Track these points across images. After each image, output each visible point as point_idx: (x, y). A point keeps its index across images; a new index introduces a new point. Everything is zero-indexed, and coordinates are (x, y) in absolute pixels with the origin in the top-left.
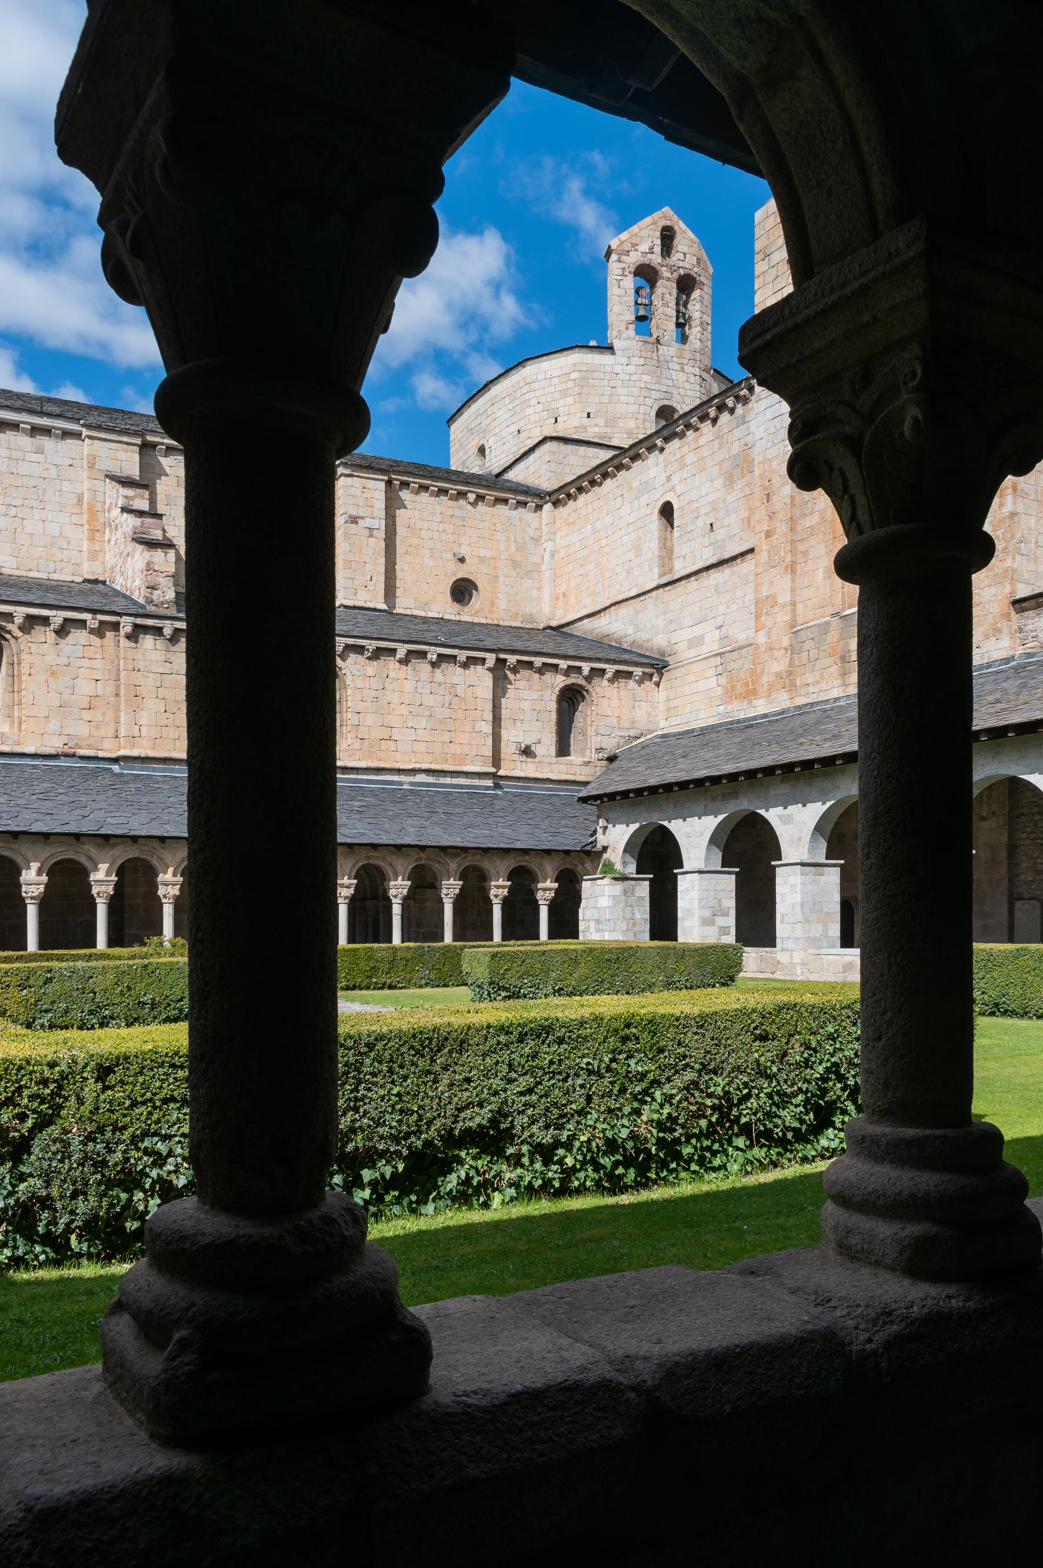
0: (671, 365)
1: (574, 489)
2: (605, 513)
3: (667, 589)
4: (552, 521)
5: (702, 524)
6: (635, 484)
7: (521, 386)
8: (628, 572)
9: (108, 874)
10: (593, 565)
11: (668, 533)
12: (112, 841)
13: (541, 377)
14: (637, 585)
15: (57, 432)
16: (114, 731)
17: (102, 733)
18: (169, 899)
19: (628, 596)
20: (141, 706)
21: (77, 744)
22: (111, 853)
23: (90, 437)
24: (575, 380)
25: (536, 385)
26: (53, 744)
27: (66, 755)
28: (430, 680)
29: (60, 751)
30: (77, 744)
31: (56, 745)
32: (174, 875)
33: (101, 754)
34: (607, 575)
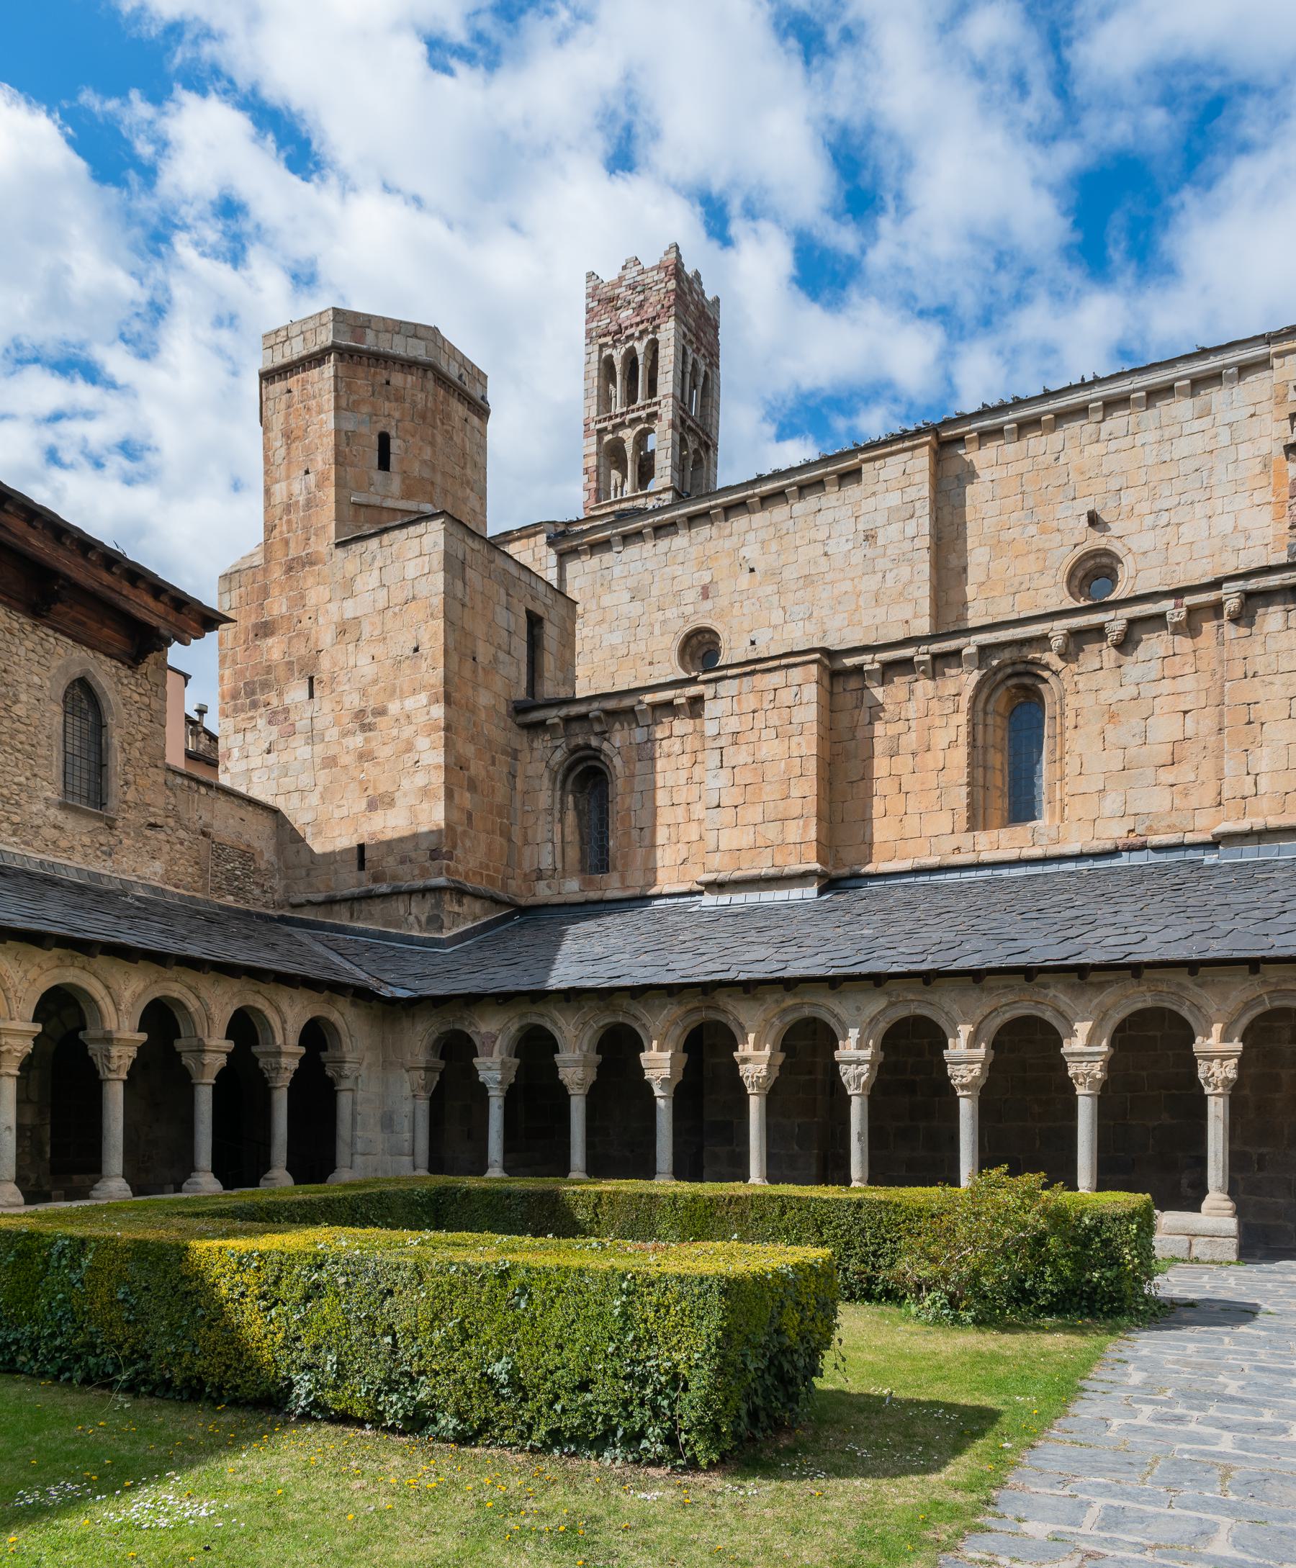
9: (1091, 1040)
12: (1094, 977)
15: (1230, 371)
16: (1214, 794)
17: (1194, 801)
18: (1216, 1087)
20: (1259, 739)
21: (1150, 828)
22: (1096, 1001)
23: (1280, 355)
26: (1113, 833)
27: (1131, 849)
29: (1120, 843)
30: (1150, 828)
31: (1116, 835)
32: (1225, 1038)
33: (1189, 838)
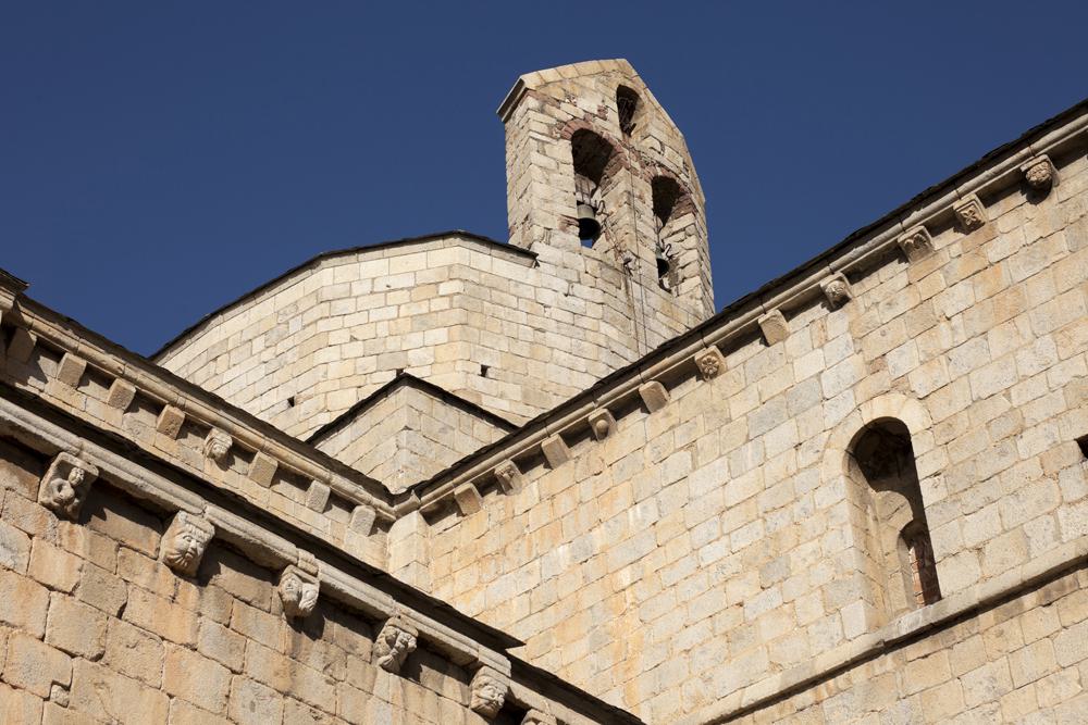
0: (652, 323)
1: (509, 462)
2: (623, 501)
3: (911, 651)
4: (422, 559)
5: (1043, 445)
6: (737, 409)
7: (302, 309)
8: (731, 637)
10: (583, 646)
11: (871, 521)
13: (367, 287)
14: (775, 666)
19: (746, 702)
24: (450, 296)
25: (349, 305)
28: (283, 684)
34: (644, 661)
